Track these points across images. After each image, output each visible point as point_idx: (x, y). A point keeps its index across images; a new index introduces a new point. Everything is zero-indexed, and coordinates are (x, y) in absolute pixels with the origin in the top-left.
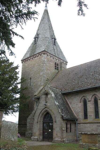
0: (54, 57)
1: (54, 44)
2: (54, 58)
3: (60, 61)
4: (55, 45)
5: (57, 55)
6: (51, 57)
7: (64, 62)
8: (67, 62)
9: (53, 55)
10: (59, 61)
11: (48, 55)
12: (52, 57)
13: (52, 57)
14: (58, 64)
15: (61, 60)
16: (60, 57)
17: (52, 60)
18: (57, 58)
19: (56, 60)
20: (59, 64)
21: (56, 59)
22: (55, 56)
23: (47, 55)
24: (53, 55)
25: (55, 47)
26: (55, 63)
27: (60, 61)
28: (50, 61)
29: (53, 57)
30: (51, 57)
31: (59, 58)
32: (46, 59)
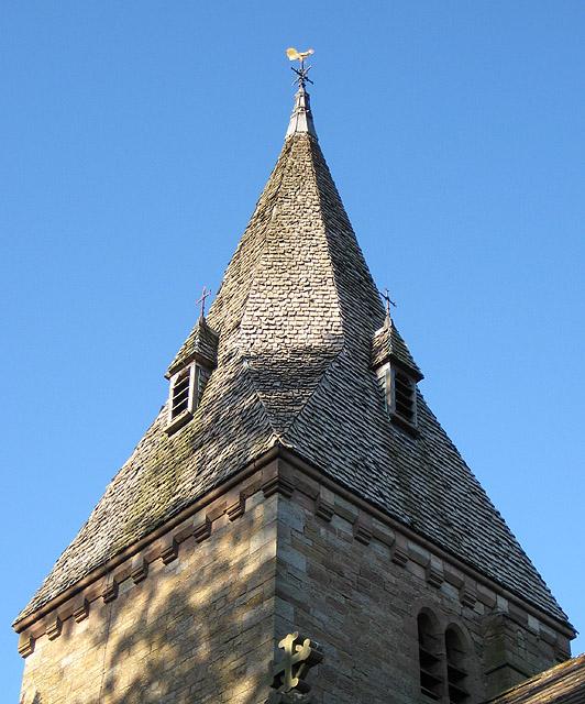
0: (404, 544)
1: (395, 421)
2: (399, 561)
3: (479, 608)
4: (414, 434)
5: (431, 528)
6: (363, 537)
7: (533, 623)
8: (568, 632)
9: (393, 522)
10: (467, 602)
11: (324, 514)
12: (379, 539)
13: (379, 539)
14: (452, 635)
15: (498, 587)
16: (476, 547)
17: (376, 578)
18: (437, 564)
19: (434, 581)
20: (469, 639)
21: (426, 567)
22: (412, 531)
23: (308, 503)
24: (393, 522)
25: (411, 448)
26: (425, 619)
27: (479, 608)
28: (361, 587)
29: (390, 545)
30: (363, 537)
31: (470, 569)
32: (305, 551)
